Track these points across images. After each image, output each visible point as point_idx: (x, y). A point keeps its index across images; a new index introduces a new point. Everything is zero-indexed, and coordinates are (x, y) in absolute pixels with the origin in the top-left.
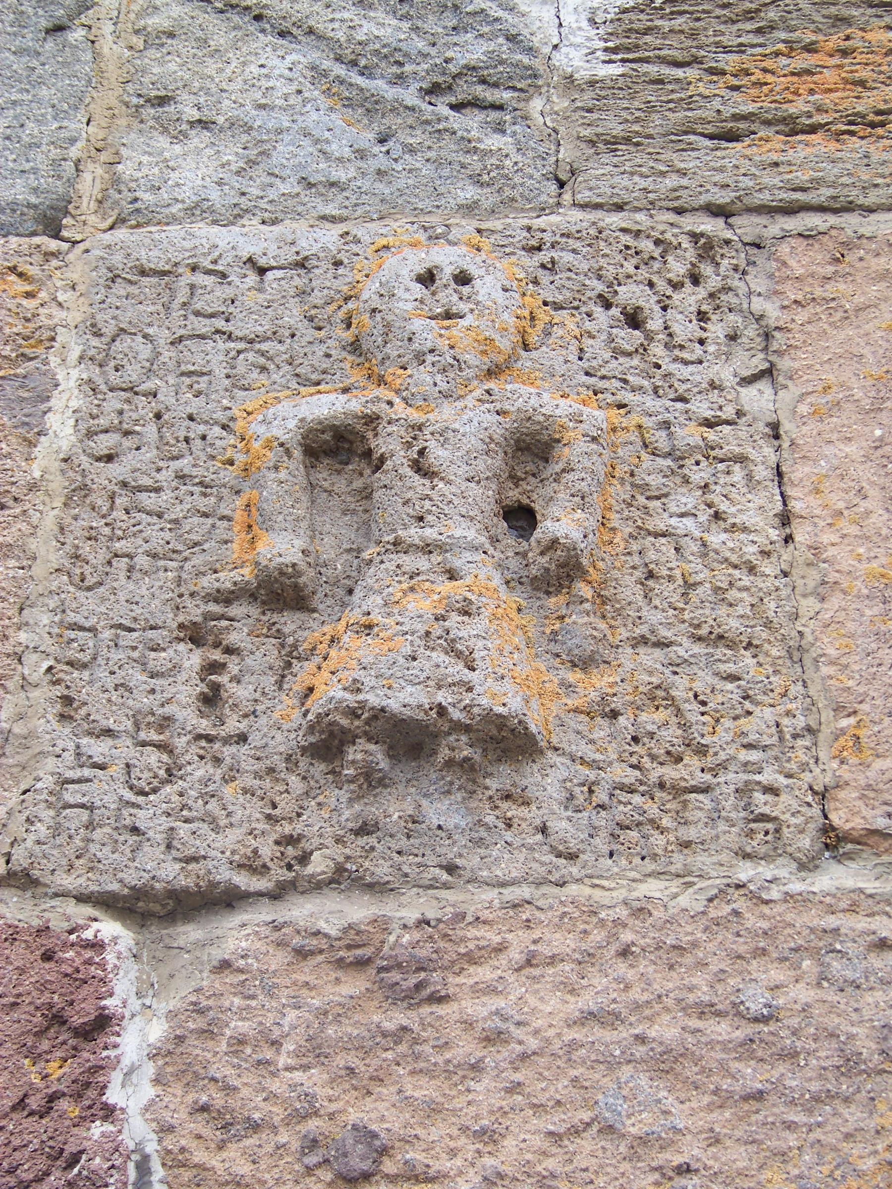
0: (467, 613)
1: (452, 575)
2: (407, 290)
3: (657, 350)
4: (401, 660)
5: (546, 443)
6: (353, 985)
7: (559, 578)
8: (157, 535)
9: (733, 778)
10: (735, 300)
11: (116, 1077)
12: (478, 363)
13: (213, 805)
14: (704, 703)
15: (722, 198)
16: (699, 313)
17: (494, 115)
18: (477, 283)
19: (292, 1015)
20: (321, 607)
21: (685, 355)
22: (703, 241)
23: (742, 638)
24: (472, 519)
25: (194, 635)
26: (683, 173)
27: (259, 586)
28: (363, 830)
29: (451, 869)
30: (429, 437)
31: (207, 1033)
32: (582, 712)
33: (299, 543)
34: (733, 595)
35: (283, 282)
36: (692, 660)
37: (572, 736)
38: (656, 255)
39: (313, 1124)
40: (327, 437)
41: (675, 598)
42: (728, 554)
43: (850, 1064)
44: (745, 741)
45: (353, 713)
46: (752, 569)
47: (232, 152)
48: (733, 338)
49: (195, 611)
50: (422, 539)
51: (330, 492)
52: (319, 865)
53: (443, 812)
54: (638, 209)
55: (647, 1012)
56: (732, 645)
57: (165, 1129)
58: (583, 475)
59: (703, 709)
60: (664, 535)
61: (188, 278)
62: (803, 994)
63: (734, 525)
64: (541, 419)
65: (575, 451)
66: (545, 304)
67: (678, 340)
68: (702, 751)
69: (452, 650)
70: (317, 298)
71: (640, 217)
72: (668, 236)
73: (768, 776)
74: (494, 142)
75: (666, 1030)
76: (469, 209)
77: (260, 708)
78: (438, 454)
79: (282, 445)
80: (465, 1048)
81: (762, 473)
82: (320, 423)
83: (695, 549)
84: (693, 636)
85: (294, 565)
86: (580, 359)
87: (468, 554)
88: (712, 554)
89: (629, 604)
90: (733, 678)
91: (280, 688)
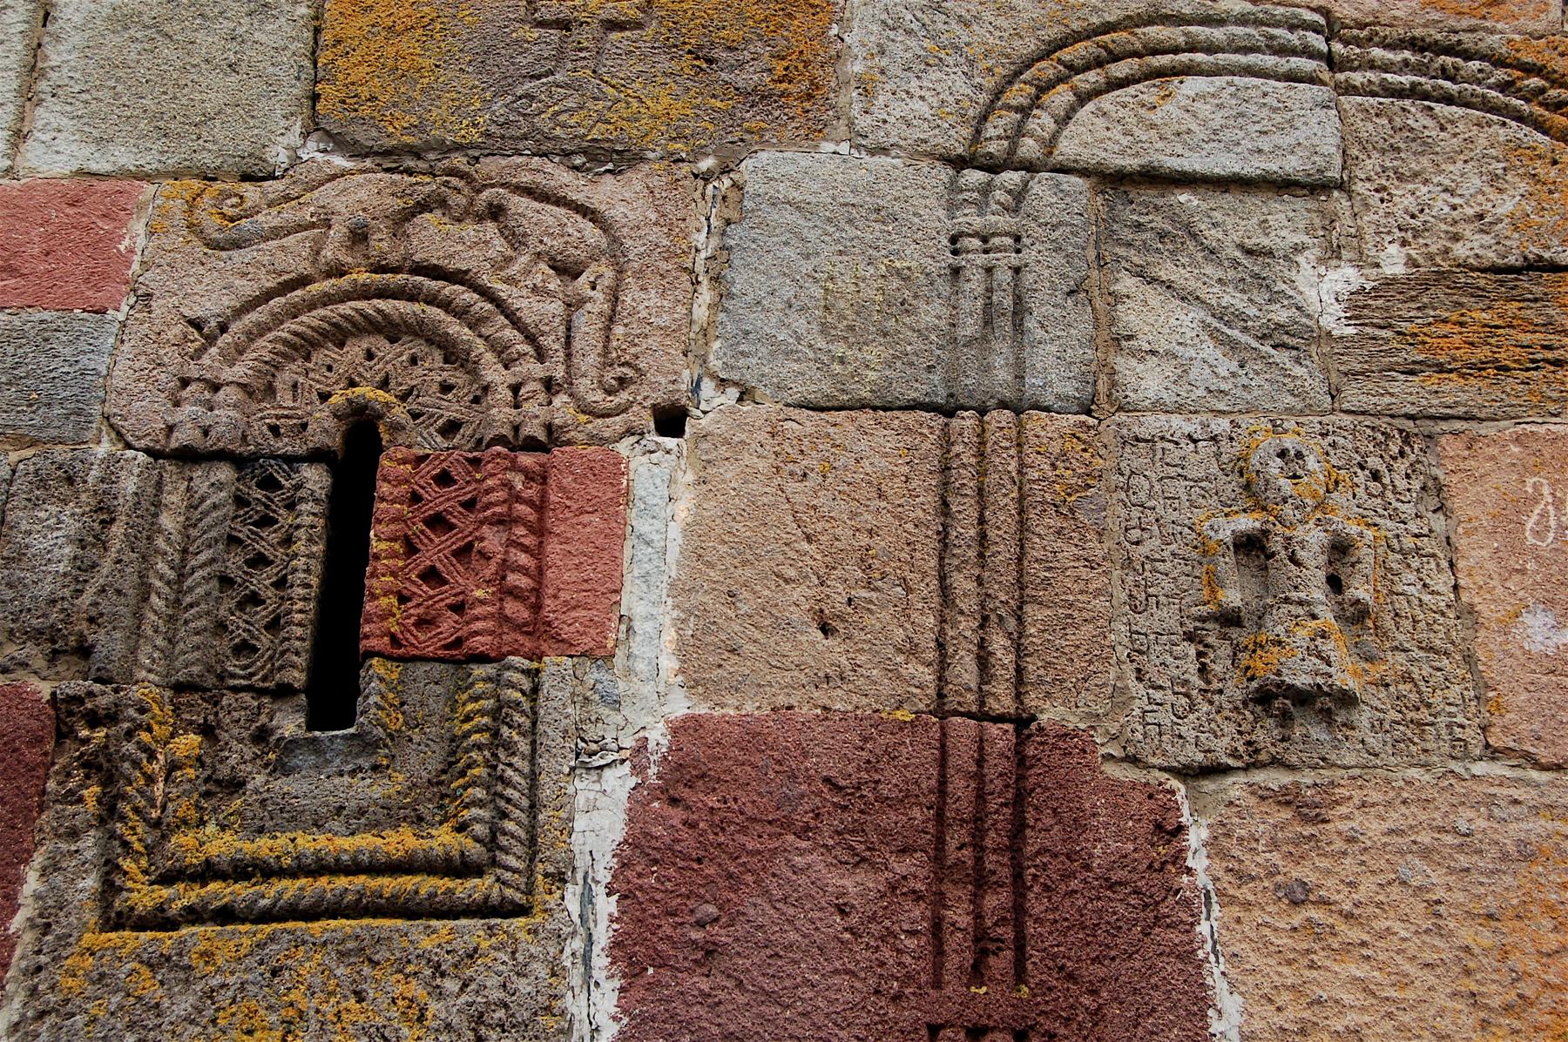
0: (1323, 637)
1: (1314, 617)
3: (1389, 494)
6: (1286, 814)
8: (1167, 585)
11: (1190, 854)
13: (1213, 725)
15: (1412, 410)
17: (1294, 353)
19: (1262, 827)
25: (1190, 637)
26: (1392, 395)
28: (1283, 740)
29: (1323, 759)
31: (1228, 835)
39: (1279, 878)
43: (1505, 857)
45: (1278, 686)
46: (1443, 614)
49: (1190, 626)
52: (1263, 757)
53: (1317, 732)
57: (1216, 879)
61: (1159, 445)
68: (1429, 706)
69: (1319, 656)
70: (1225, 458)
73: (1460, 719)
74: (1298, 371)
75: (1425, 838)
78: (1301, 555)
80: (1339, 845)
81: (1444, 564)
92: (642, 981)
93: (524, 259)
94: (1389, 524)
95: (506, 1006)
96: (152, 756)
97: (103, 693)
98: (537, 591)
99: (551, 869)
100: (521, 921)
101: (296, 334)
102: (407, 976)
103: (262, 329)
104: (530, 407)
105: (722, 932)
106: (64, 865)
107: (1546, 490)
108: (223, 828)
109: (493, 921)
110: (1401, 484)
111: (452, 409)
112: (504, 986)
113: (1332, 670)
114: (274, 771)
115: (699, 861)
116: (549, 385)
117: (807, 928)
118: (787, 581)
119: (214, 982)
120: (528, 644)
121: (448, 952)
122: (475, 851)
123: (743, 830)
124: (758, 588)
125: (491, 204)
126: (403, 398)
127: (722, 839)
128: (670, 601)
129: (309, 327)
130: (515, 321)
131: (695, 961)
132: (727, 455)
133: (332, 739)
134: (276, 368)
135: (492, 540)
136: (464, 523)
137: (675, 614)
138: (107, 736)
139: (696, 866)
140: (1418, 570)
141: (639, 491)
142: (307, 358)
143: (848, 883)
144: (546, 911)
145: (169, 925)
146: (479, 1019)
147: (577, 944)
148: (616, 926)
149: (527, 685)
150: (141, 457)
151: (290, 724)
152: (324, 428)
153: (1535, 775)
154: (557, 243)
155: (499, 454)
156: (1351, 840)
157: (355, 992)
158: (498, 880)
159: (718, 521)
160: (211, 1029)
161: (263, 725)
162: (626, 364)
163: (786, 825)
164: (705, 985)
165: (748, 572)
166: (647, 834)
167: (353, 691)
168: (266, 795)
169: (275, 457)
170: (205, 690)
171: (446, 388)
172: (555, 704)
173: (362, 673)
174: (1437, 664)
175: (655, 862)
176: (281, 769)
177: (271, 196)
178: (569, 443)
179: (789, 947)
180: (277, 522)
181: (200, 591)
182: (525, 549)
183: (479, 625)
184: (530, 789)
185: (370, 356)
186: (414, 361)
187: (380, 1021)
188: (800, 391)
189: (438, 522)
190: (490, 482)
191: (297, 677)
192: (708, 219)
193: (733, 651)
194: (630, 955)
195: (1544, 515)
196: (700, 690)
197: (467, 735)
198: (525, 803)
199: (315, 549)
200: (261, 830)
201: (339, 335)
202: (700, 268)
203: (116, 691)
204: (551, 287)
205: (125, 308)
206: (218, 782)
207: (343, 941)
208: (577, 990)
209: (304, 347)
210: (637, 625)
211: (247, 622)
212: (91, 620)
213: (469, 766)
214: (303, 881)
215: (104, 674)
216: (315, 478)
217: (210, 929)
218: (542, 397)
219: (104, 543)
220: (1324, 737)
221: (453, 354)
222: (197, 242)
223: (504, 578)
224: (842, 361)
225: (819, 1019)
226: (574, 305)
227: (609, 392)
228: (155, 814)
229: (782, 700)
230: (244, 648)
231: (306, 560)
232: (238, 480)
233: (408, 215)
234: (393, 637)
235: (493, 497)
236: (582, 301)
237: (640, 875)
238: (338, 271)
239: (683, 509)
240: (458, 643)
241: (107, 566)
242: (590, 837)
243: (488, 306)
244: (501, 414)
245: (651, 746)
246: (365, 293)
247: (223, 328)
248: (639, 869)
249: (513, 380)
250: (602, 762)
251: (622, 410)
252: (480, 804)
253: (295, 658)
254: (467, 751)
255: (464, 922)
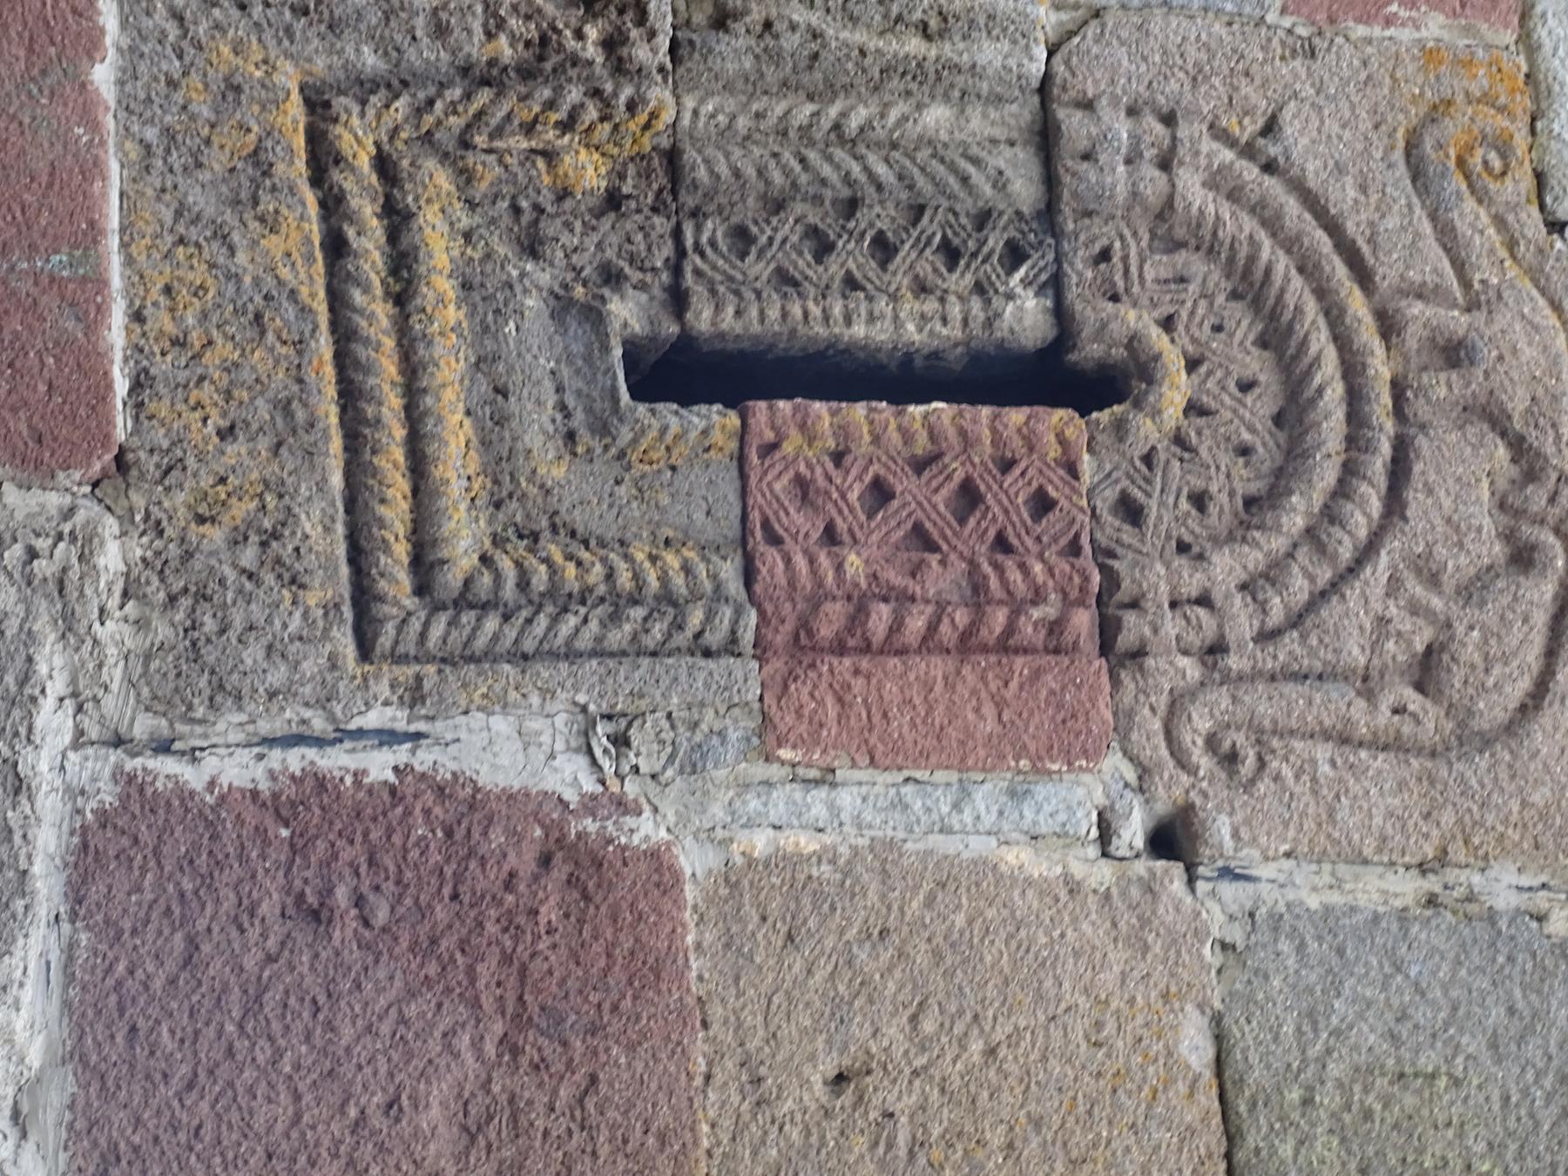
92: (269, 821)
93: (1437, 603)
95: (223, 631)
96: (566, 126)
97: (654, 51)
98: (866, 648)
99: (427, 685)
100: (349, 649)
101: (1268, 272)
102: (261, 496)
103: (1272, 223)
104: (1172, 626)
105: (349, 933)
106: (393, 24)
108: (468, 236)
109: (348, 612)
111: (1165, 512)
112: (251, 628)
114: (557, 297)
115: (455, 896)
116: (1216, 649)
117: (361, 1053)
118: (914, 1019)
119: (236, 237)
120: (781, 638)
121: (297, 549)
122: (452, 578)
123: (506, 959)
124: (898, 974)
125: (1533, 548)
126: (1179, 440)
127: (491, 928)
128: (866, 842)
129: (1282, 291)
130: (1321, 597)
131: (302, 895)
132: (1122, 925)
133: (610, 370)
134: (1211, 250)
135: (942, 579)
136: (974, 538)
137: (844, 850)
138: (590, 63)
139: (447, 891)
141: (1042, 790)
142: (1235, 295)
143: (435, 1111)
144: (365, 679)
145: (318, 177)
146: (203, 596)
147: (319, 724)
148: (349, 780)
149: (714, 639)
150: (1037, 68)
151: (628, 312)
152: (1115, 324)
154: (1470, 652)
155: (1086, 579)
157: (232, 427)
158: (409, 614)
159: (1005, 913)
160: (169, 239)
161: (626, 278)
162: (1262, 763)
163: (520, 1020)
164: (268, 909)
165: (922, 959)
166: (490, 820)
167: (687, 398)
168: (518, 289)
169: (1058, 260)
170: (674, 193)
171: (1200, 500)
172: (683, 678)
173: (717, 407)
175: (449, 833)
176: (561, 305)
177: (1511, 218)
178: (1115, 682)
179: (330, 1026)
180: (951, 270)
181: (827, 171)
182: (932, 627)
183: (800, 562)
184: (550, 653)
185: (1246, 386)
186: (1244, 451)
187: (191, 462)
188: (1245, 1035)
189: (969, 497)
190: (1038, 568)
191: (702, 318)
192: (1544, 886)
193: (790, 937)
194: (304, 808)
196: (724, 891)
197: (627, 557)
198: (529, 645)
199: (911, 327)
200: (466, 286)
201: (1277, 337)
202: (1451, 875)
203: (661, 69)
204: (1390, 645)
205: (1287, 22)
206: (536, 222)
207: (305, 405)
208: (250, 728)
209: (1250, 286)
210: (822, 793)
211: (784, 241)
212: (768, 25)
213: (579, 564)
214: (389, 343)
215: (684, 51)
216: (1024, 315)
217: (315, 230)
218: (1194, 640)
219: (892, 30)
221: (1257, 508)
222: (1416, 113)
223: (885, 600)
224: (1307, 1102)
225: (224, 1071)
226: (1367, 684)
227: (1212, 742)
228: (480, 140)
229: (716, 1011)
230: (742, 238)
231: (895, 322)
232: (1018, 213)
233: (1497, 421)
234: (773, 447)
235: (1015, 576)
236: (1369, 695)
237: (427, 812)
238: (1388, 326)
239: (1017, 857)
240: (774, 540)
241: (859, 37)
242: (480, 739)
243: (1346, 553)
244: (1157, 578)
245: (630, 821)
246: (1352, 369)
247: (1269, 167)
248: (438, 811)
249: (1217, 597)
250: (598, 752)
251: (1183, 762)
252: (523, 584)
253: (730, 310)
254: (604, 560)
255: (345, 570)
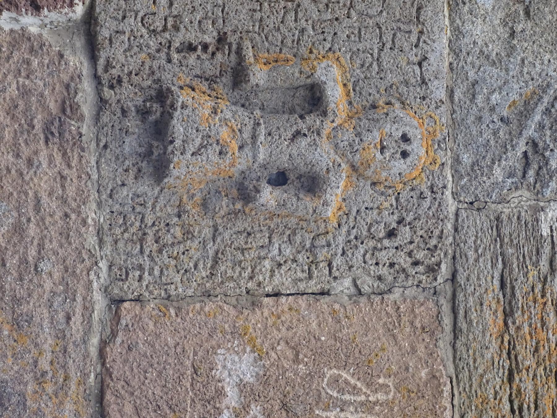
0: (220, 153)
1: (241, 148)
2: (397, 129)
3: (372, 243)
4: (196, 126)
5: (314, 190)
6: (53, 106)
7: (244, 194)
8: (270, 22)
9: (147, 264)
10: (400, 280)
11: (14, 15)
12: (356, 160)
13: (136, 49)
14: (184, 253)
15: (461, 279)
16: (394, 264)
17: (520, 174)
18: (402, 161)
19: (41, 83)
20: (235, 93)
21: (368, 256)
22: (436, 268)
23: (215, 271)
24: (270, 156)
25: (221, 39)
26: (477, 260)
27: (242, 66)
28: (124, 112)
29: (106, 147)
30: (313, 138)
31: (32, 50)
32: (180, 203)
33: (262, 82)
34: (238, 269)
35: (412, 73)
36: (205, 250)
37: (168, 198)
38: (428, 246)
40: (318, 94)
41: (236, 244)
42: (258, 268)
44: (164, 270)
45: (172, 106)
46: (251, 278)
47: (494, 49)
48: (380, 278)
49: (233, 39)
50: (259, 135)
51: (293, 96)
53: (131, 144)
54: (454, 238)
55: (41, 223)
56: (212, 267)
58: (295, 205)
59: (180, 253)
60: (270, 241)
61: (415, 30)
62: (48, 285)
63: (274, 271)
64: (325, 188)
65: (308, 202)
66: (399, 194)
67: (377, 253)
68: (160, 251)
69: (202, 146)
70: (403, 89)
71: (451, 239)
72: (438, 252)
75: (32, 230)
76: (457, 160)
77: (184, 68)
78: (303, 142)
79: (312, 74)
80: (26, 152)
81: (302, 286)
82: (324, 91)
83: (262, 254)
84: (218, 251)
85: (249, 81)
86: (367, 208)
87: (251, 154)
88: (259, 261)
89: (234, 225)
90: (196, 266)
91: (195, 76)
94: (341, 239)
107: (381, 396)
110: (383, 256)
113: (188, 156)
140: (294, 261)
153: (95, 341)
156: (30, 162)
174: (201, 266)
195: (355, 390)
220: (127, 149)
